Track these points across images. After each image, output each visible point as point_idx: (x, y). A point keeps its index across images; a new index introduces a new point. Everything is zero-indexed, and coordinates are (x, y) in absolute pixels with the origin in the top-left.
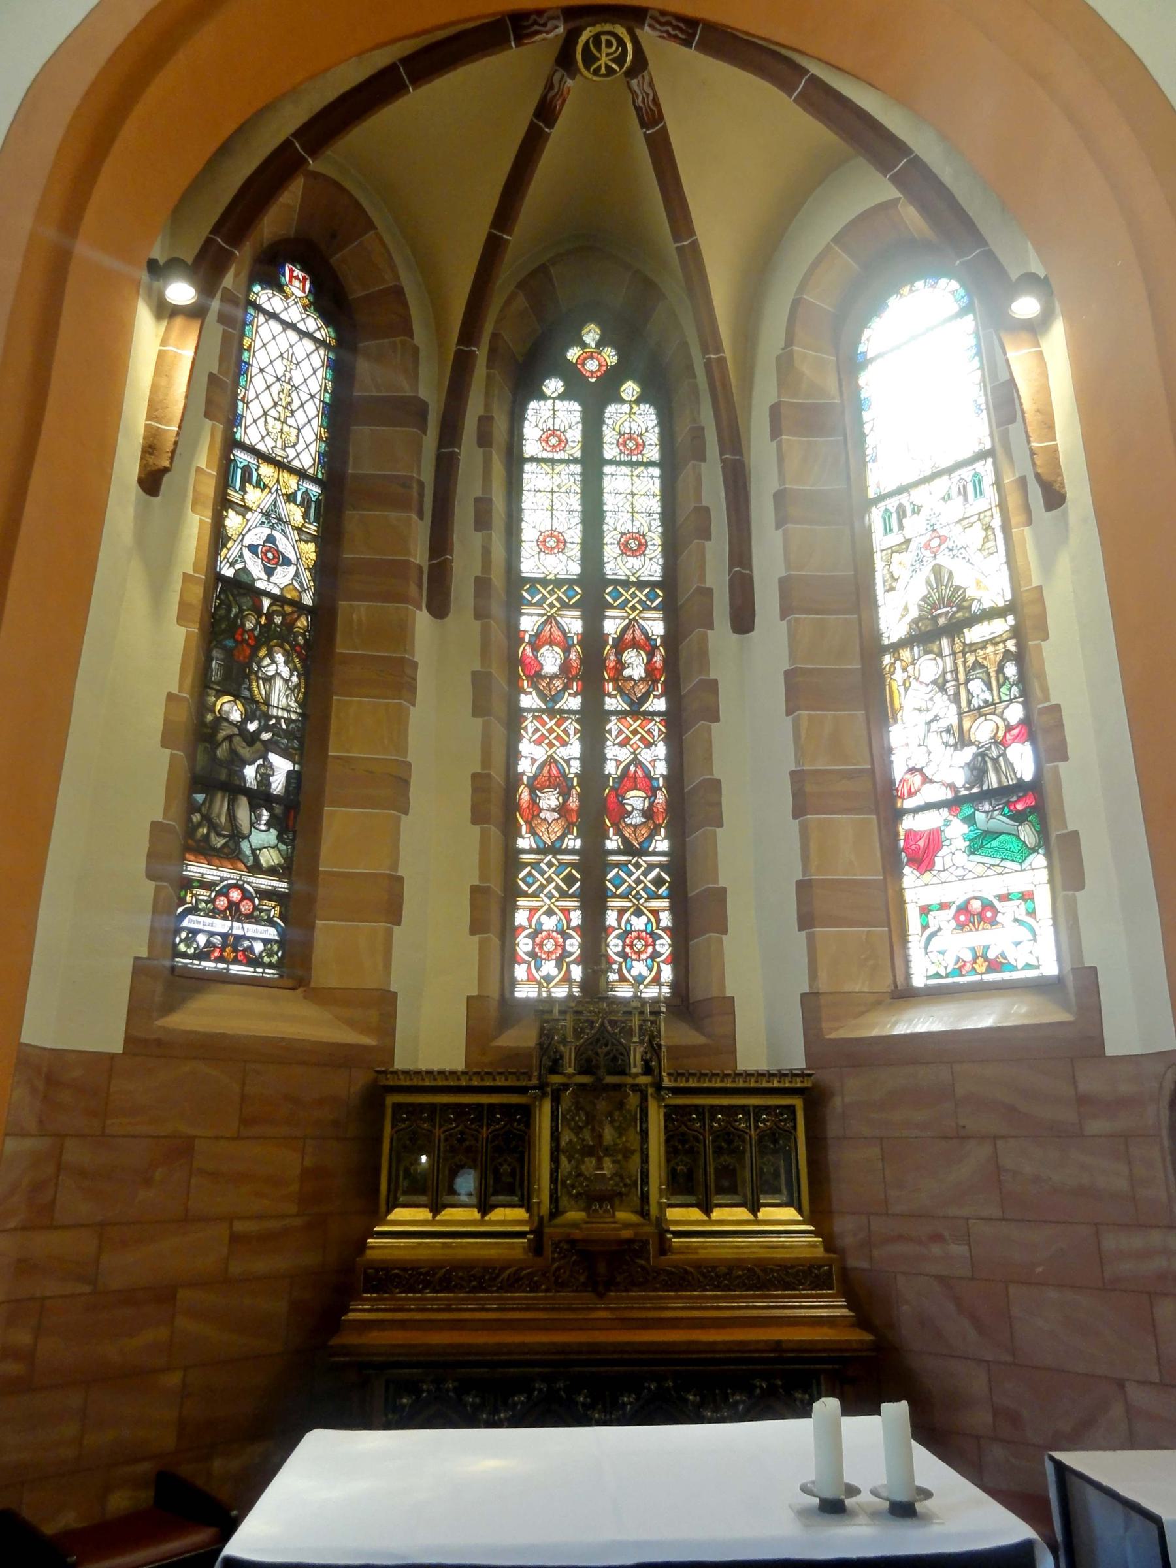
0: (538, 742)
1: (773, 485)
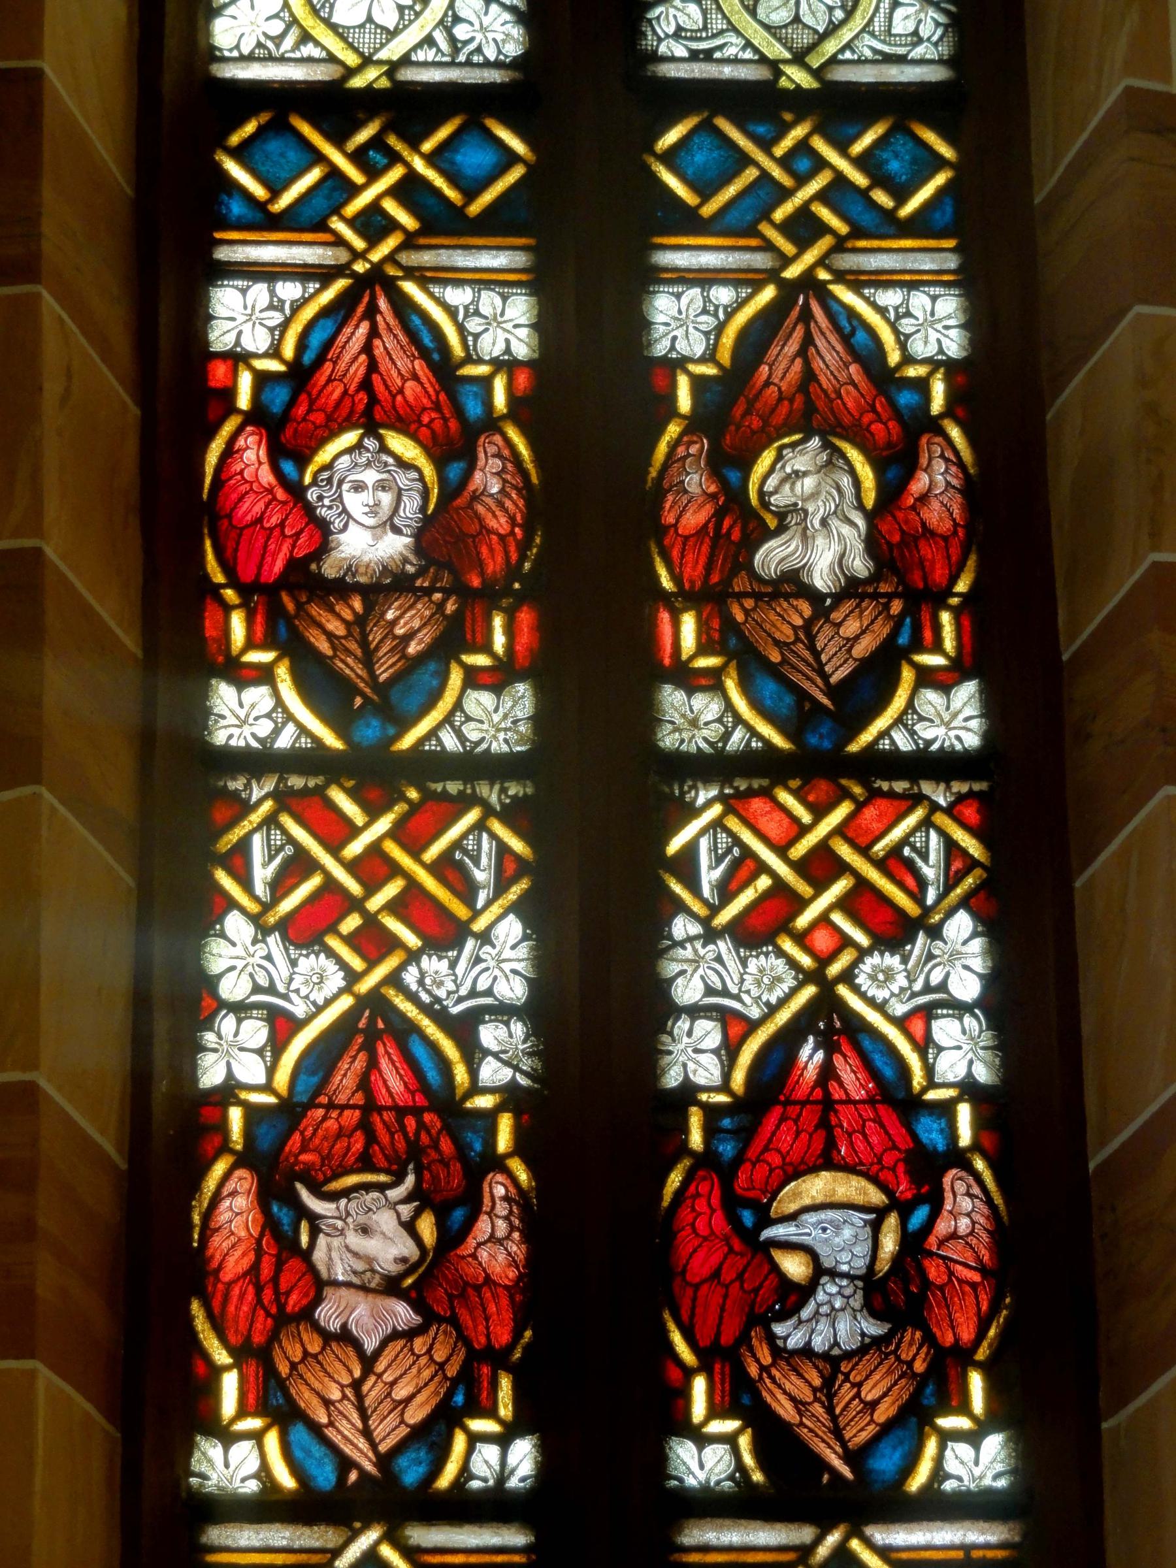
0: (306, 931)
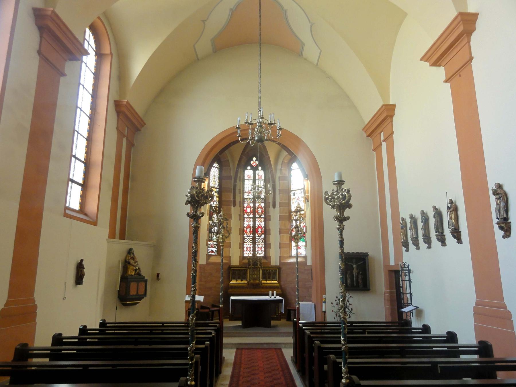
1: (278, 188)
